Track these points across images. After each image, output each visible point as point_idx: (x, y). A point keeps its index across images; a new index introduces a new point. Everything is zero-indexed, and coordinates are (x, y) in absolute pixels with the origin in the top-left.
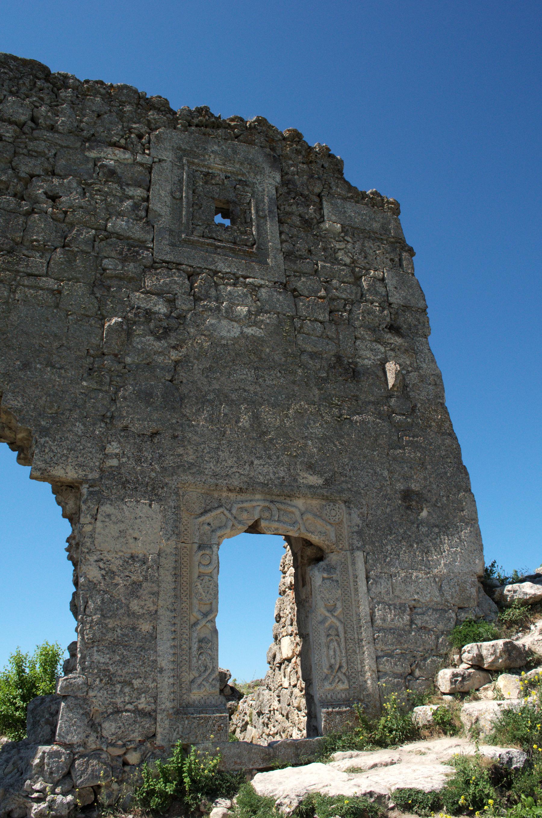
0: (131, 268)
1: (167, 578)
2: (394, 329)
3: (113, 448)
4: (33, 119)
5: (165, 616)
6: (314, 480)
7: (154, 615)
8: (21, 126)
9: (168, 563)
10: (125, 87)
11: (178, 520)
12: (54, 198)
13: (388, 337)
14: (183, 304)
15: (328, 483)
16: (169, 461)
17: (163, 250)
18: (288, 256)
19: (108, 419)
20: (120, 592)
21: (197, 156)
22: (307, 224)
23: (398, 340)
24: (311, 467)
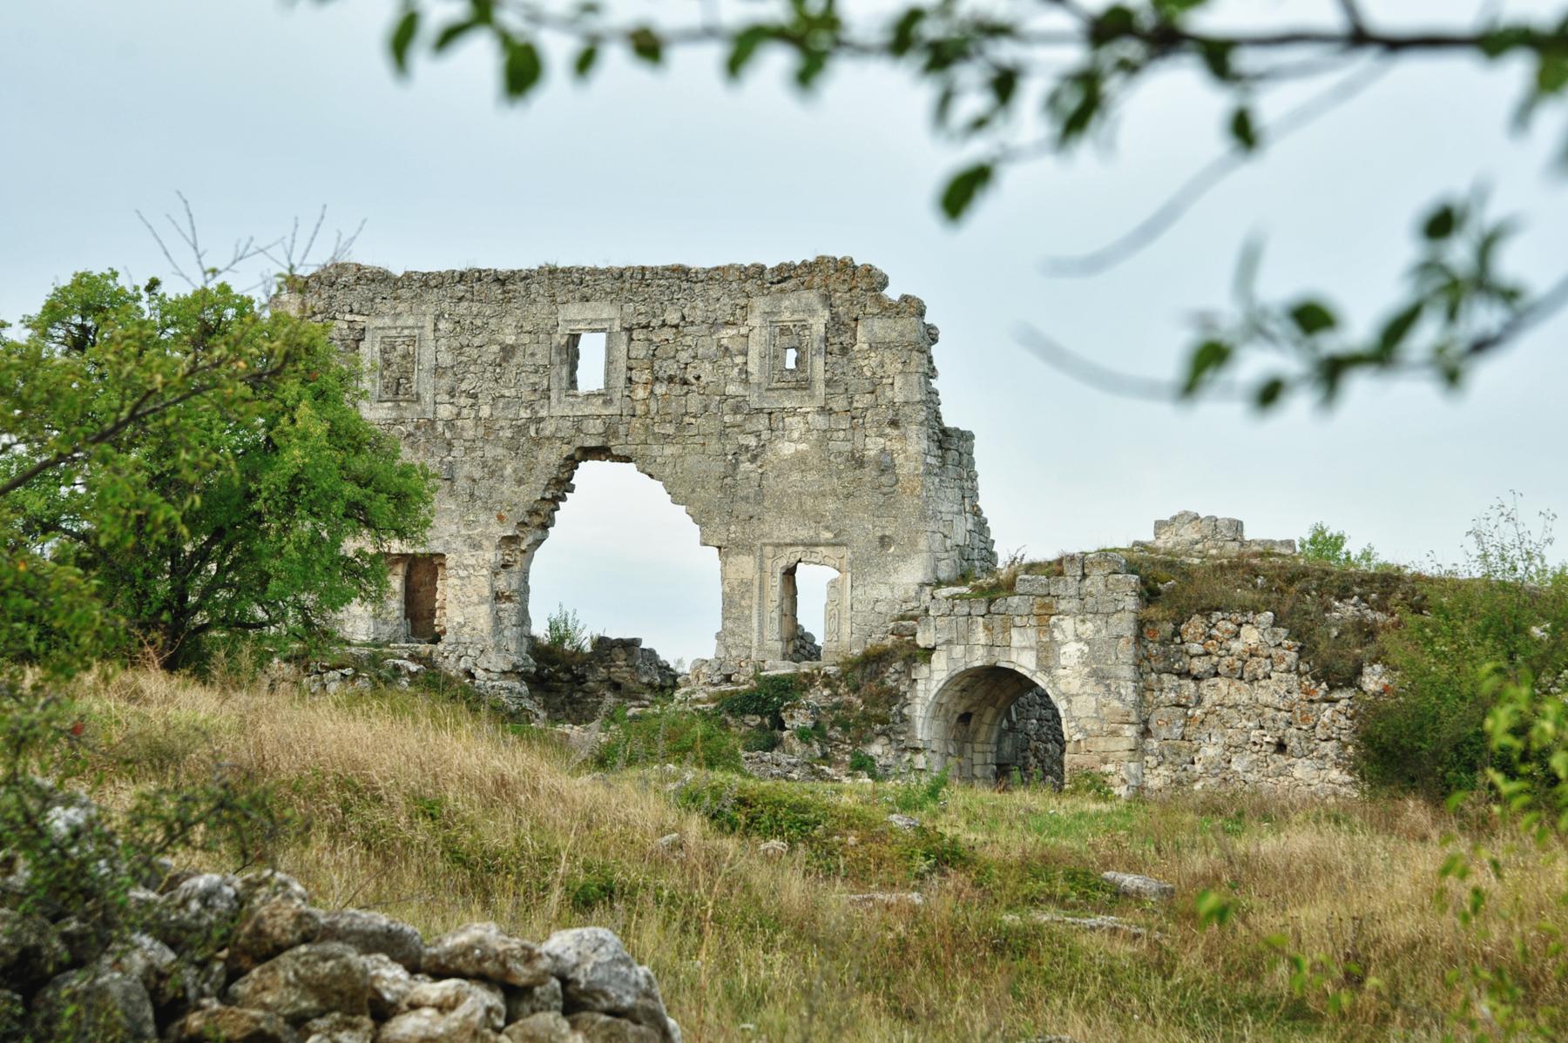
0: (739, 418)
1: (756, 590)
2: (894, 423)
3: (733, 528)
4: (683, 318)
5: (755, 607)
6: (828, 535)
7: (750, 607)
8: (676, 326)
9: (756, 583)
10: (731, 266)
11: (762, 562)
12: (698, 378)
13: (888, 430)
14: (765, 435)
15: (836, 536)
16: (758, 533)
17: (754, 401)
18: (828, 383)
19: (730, 514)
20: (737, 598)
21: (775, 314)
22: (844, 351)
23: (896, 432)
24: (827, 528)
